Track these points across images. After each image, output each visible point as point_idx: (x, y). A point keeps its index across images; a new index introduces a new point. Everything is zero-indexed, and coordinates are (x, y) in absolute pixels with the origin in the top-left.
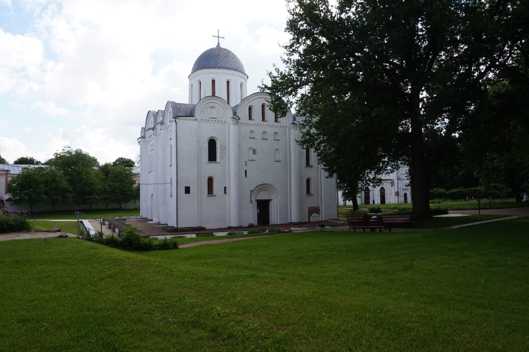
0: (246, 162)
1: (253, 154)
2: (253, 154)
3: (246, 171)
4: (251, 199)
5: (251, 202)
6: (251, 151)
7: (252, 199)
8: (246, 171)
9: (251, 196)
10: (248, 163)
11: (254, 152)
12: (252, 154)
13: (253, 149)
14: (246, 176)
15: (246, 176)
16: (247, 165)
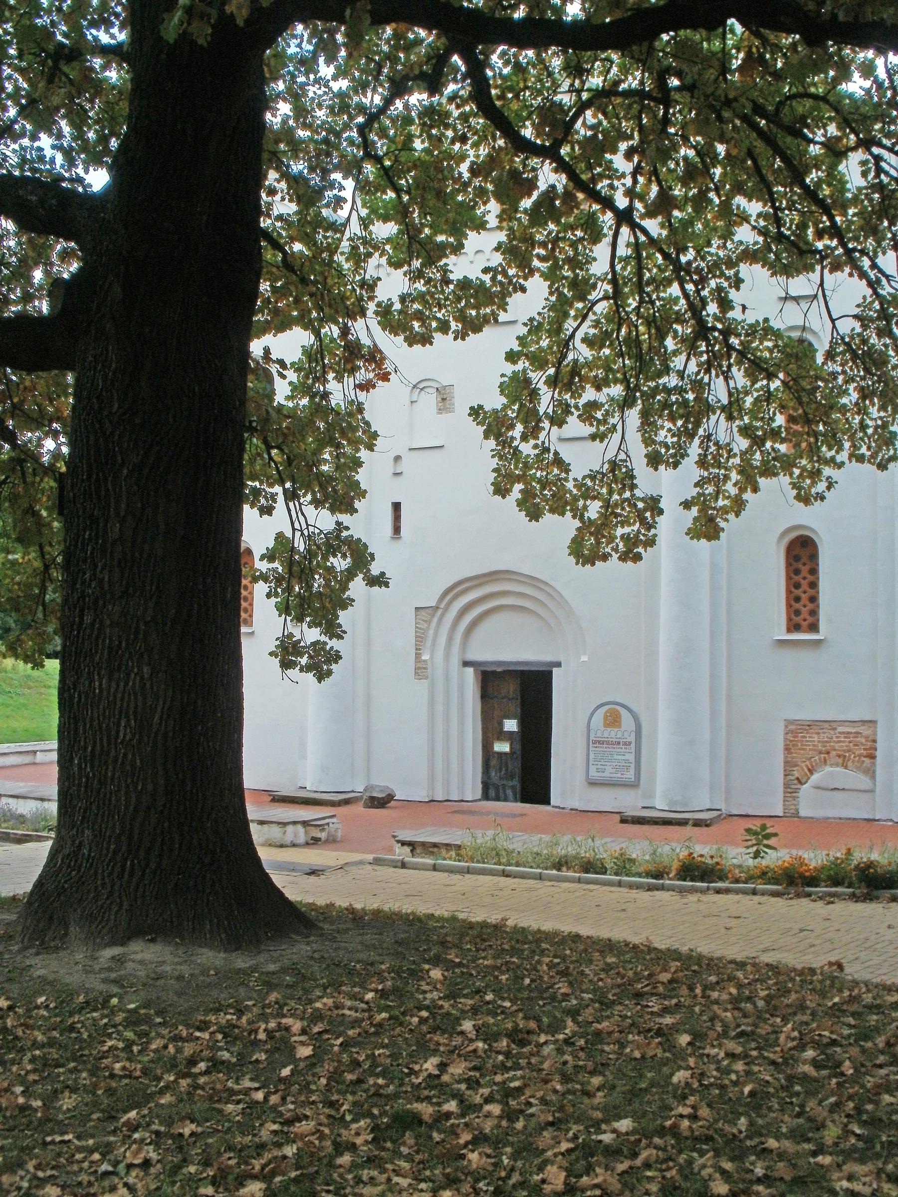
0: (397, 458)
1: (440, 411)
2: (440, 411)
3: (397, 507)
4: (418, 656)
5: (421, 670)
6: (430, 400)
7: (424, 657)
8: (397, 507)
9: (420, 639)
10: (409, 463)
11: (444, 399)
12: (434, 409)
13: (436, 385)
14: (397, 530)
15: (397, 530)
16: (397, 474)
